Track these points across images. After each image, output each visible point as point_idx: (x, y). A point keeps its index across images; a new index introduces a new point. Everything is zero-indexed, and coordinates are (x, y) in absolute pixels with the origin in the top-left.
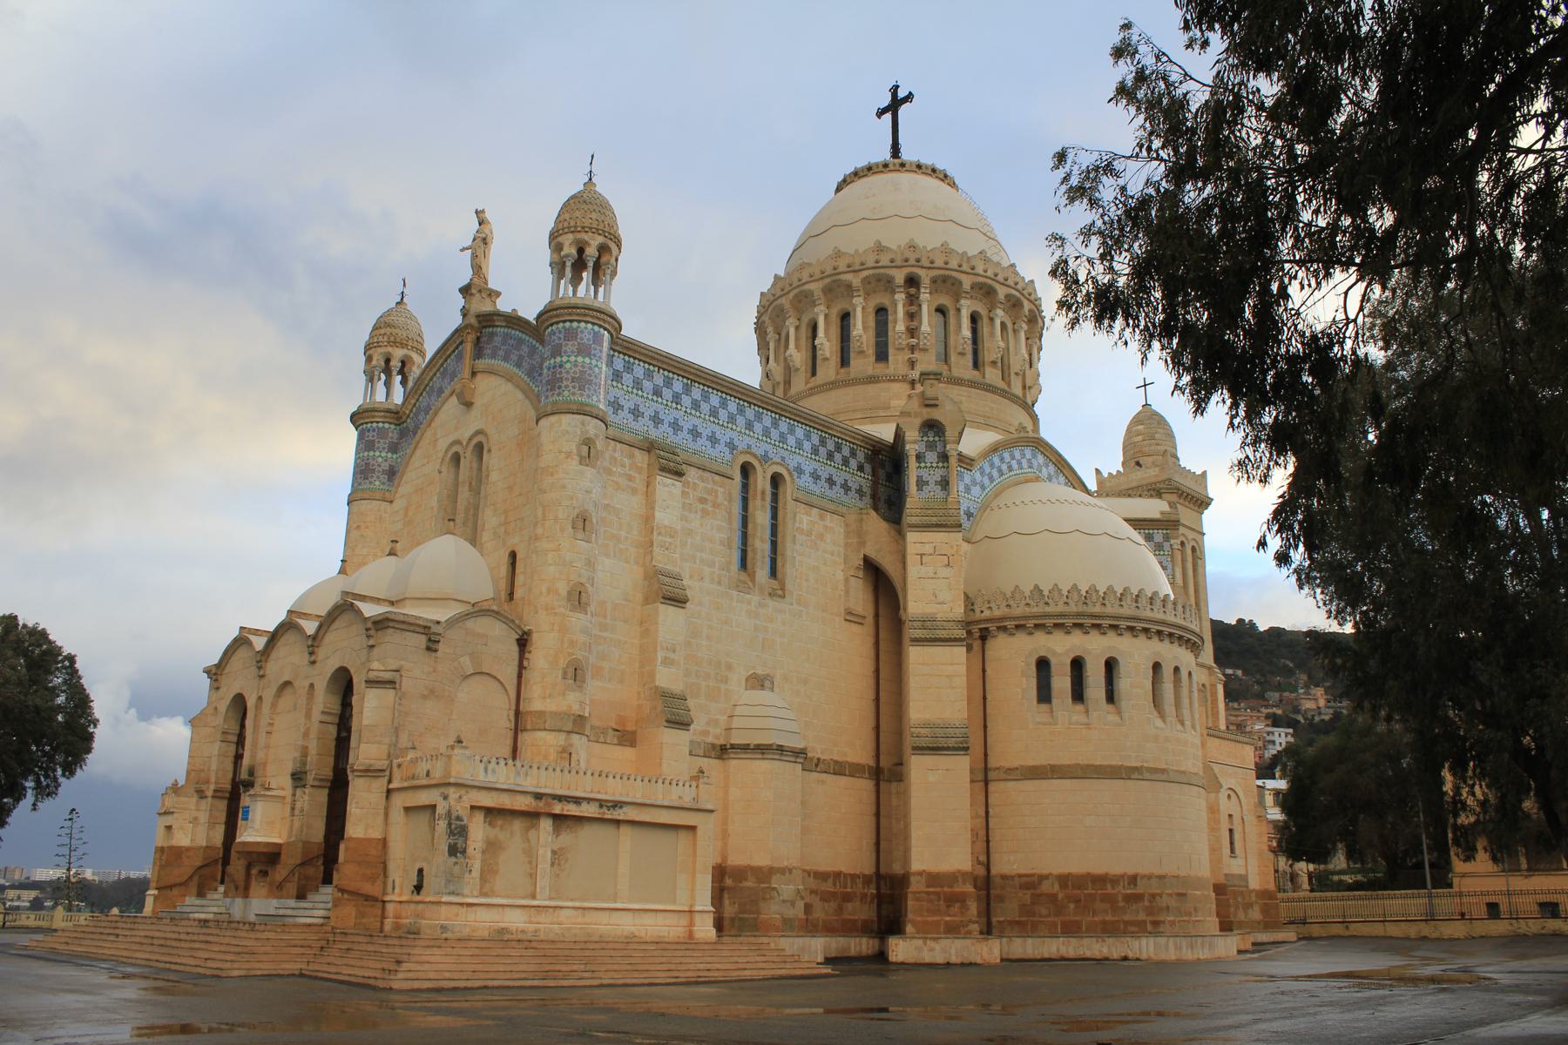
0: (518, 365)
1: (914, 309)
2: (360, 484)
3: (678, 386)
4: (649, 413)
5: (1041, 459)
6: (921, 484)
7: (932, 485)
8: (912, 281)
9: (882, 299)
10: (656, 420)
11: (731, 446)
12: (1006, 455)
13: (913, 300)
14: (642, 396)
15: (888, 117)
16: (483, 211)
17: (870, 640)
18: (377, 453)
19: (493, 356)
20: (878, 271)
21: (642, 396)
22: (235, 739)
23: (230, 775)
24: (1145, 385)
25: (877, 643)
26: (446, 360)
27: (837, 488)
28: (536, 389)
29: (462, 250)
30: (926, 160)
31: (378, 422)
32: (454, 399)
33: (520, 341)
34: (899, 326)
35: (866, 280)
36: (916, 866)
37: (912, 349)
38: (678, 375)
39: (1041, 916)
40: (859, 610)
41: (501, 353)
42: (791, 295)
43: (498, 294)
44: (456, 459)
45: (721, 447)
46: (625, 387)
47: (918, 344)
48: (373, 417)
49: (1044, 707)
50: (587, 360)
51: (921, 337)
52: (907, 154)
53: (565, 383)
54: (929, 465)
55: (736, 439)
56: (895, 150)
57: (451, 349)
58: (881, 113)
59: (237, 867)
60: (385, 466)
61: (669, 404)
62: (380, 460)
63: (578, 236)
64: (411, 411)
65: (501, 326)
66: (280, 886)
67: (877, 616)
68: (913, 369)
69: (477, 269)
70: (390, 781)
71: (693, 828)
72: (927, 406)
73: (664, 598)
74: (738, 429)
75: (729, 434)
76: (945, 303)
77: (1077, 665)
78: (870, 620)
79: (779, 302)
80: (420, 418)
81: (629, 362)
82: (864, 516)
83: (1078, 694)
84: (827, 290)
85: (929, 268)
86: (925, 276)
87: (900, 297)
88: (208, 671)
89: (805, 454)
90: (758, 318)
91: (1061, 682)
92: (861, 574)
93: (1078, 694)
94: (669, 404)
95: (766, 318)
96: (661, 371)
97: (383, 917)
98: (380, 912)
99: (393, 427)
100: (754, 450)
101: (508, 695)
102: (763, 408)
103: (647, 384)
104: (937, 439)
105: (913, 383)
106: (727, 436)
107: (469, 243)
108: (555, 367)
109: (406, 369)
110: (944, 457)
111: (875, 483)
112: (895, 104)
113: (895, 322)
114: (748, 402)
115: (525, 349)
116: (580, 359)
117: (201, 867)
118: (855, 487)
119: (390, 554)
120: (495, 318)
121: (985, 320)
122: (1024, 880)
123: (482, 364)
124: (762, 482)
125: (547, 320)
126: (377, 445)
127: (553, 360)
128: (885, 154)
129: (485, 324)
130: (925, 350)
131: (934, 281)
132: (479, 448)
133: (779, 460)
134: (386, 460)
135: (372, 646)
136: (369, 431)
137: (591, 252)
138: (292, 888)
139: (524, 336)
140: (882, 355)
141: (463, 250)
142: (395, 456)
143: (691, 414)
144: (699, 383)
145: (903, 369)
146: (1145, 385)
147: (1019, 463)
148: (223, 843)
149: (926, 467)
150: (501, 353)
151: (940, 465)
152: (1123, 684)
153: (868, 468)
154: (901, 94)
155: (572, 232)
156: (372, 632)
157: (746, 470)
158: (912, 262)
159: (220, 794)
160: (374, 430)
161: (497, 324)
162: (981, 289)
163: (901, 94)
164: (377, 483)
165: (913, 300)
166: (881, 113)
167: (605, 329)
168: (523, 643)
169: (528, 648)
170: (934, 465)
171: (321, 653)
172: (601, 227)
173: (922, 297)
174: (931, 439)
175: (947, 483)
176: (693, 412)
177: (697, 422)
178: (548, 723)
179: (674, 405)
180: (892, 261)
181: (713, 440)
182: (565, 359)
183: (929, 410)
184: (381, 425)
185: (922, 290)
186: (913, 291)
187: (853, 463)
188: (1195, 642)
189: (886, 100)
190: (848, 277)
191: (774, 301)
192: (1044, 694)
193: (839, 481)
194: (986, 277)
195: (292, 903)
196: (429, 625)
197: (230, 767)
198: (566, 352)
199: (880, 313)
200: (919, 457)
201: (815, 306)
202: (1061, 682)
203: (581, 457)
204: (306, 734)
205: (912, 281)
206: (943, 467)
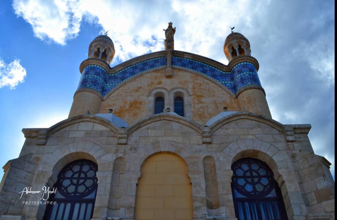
0: (204, 72)
2: (91, 86)
16: (172, 24)
18: (101, 79)
60: (102, 85)
64: (119, 71)
80: (127, 75)
107: (165, 29)
120: (186, 55)
129: (175, 55)
139: (205, 65)
141: (164, 30)
142: (106, 84)
160: (100, 70)
161: (185, 56)
164: (99, 90)
184: (103, 69)
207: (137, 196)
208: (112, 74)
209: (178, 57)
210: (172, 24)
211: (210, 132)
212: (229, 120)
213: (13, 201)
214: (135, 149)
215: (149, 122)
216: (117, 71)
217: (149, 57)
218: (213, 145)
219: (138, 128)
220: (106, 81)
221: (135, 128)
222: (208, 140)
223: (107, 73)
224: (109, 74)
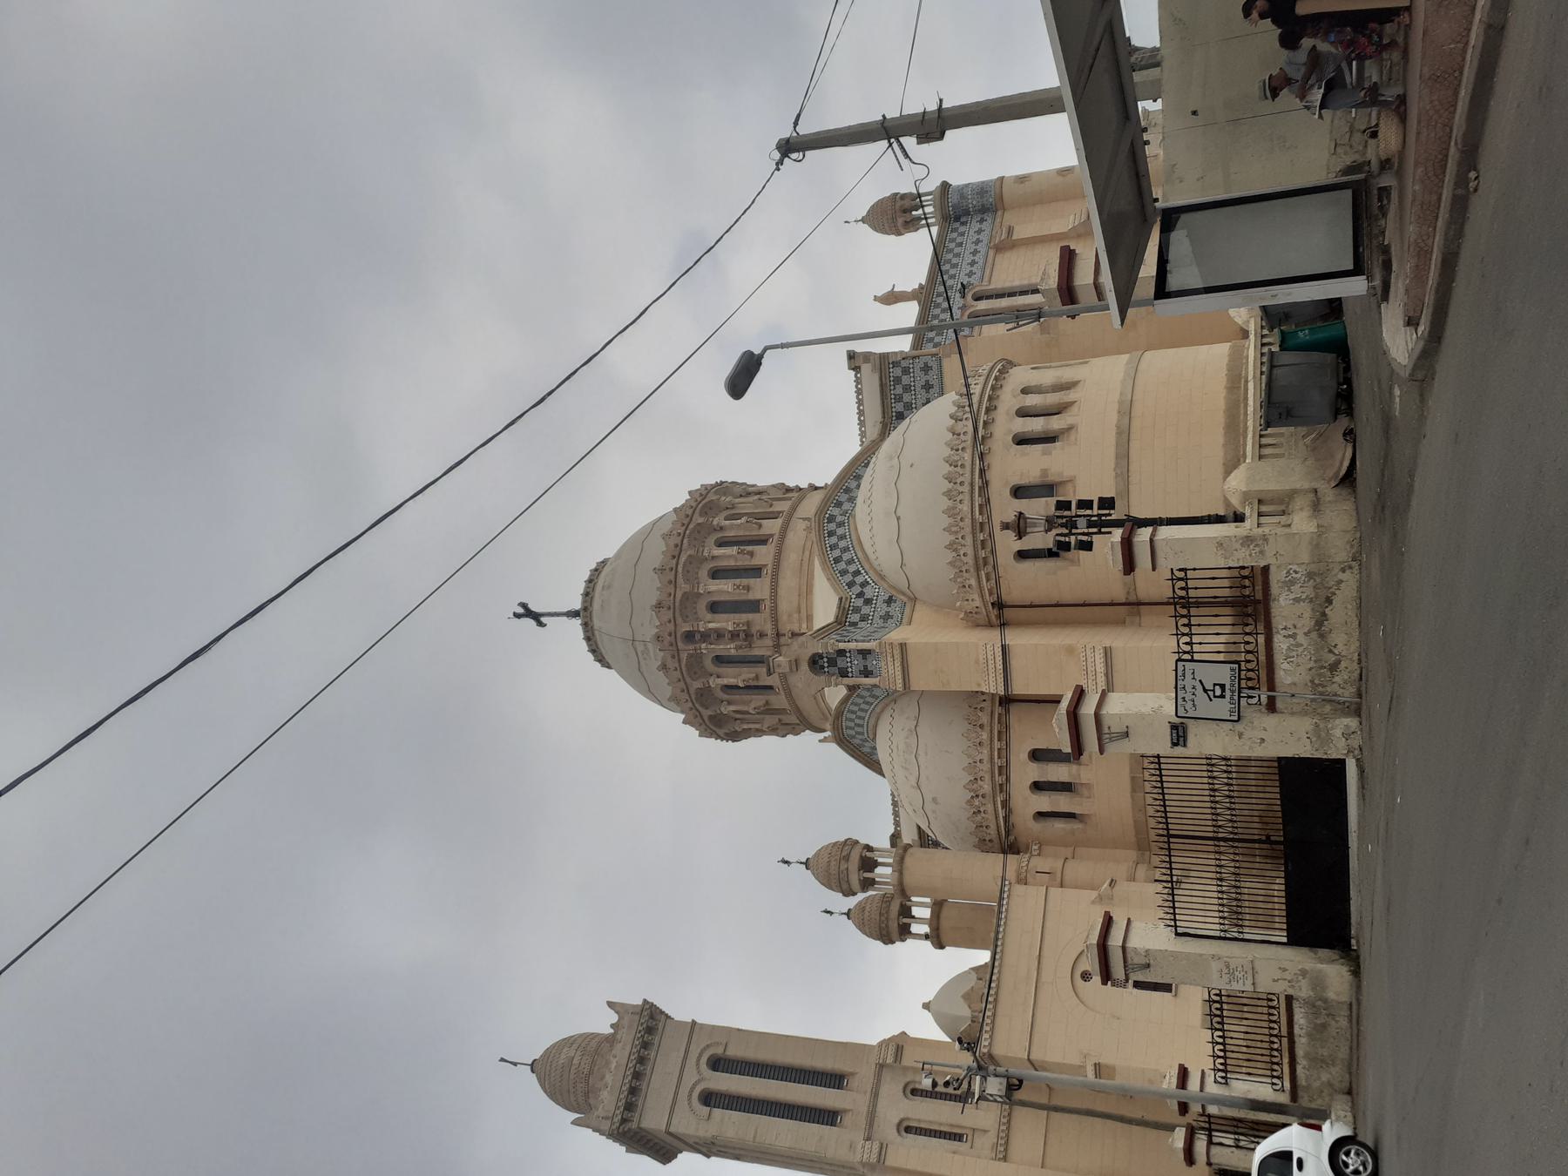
1: (713, 636)
8: (689, 637)
9: (708, 663)
30: (581, 587)
34: (730, 649)
47: (744, 631)
52: (578, 606)
54: (849, 664)
56: (574, 614)
76: (705, 604)
90: (722, 739)
95: (721, 732)
128: (577, 622)
131: (685, 619)
149: (851, 667)
165: (705, 636)
180: (673, 657)
186: (698, 637)
191: (706, 725)
201: (710, 687)
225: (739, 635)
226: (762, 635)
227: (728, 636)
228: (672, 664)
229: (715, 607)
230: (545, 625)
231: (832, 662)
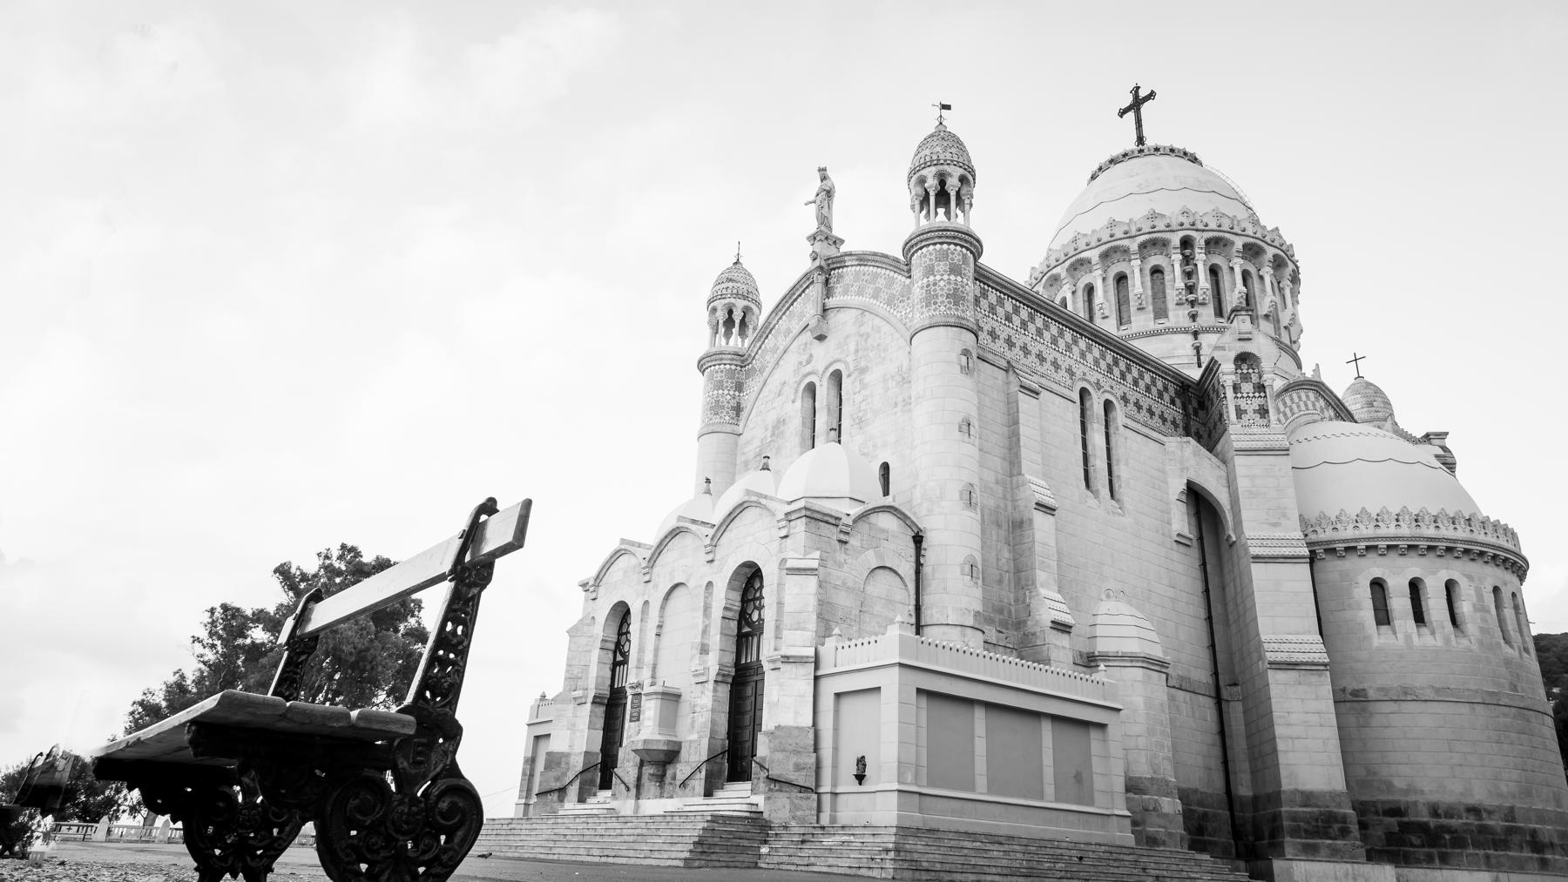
0: (875, 296)
1: (1188, 268)
3: (1024, 313)
4: (1003, 336)
5: (1322, 402)
6: (1240, 412)
7: (1250, 414)
10: (1010, 342)
11: (1070, 372)
12: (1295, 396)
13: (1187, 260)
14: (997, 321)
15: (1131, 115)
16: (824, 170)
17: (1197, 563)
18: (726, 392)
19: (846, 292)
20: (1154, 235)
21: (997, 321)
22: (612, 646)
23: (608, 682)
24: (1356, 360)
25: (1204, 564)
26: (792, 304)
27: (1156, 418)
28: (899, 315)
29: (806, 204)
31: (725, 364)
32: (808, 336)
33: (876, 276)
34: (1175, 281)
35: (1143, 246)
36: (1286, 785)
37: (1192, 303)
38: (1024, 304)
39: (1412, 845)
40: (1186, 532)
41: (855, 289)
42: (1067, 264)
43: (842, 241)
44: (811, 389)
45: (1062, 372)
46: (983, 312)
47: (1196, 299)
48: (721, 359)
49: (1384, 628)
50: (959, 279)
51: (1200, 292)
52: (1150, 142)
53: (940, 299)
54: (1245, 395)
55: (1074, 367)
56: (1140, 140)
57: (797, 294)
58: (1122, 113)
59: (627, 766)
60: (733, 403)
61: (1019, 329)
62: (728, 397)
63: (940, 167)
65: (852, 266)
66: (684, 784)
67: (1201, 539)
68: (1194, 321)
69: (824, 221)
70: (817, 668)
71: (1102, 726)
72: (1240, 340)
73: (1037, 504)
74: (1075, 358)
75: (1069, 361)
77: (1415, 586)
78: (1195, 543)
79: (1055, 271)
80: (767, 358)
81: (984, 289)
82: (1185, 445)
83: (1419, 617)
84: (1105, 256)
85: (1203, 231)
86: (1200, 239)
87: (1177, 257)
88: (584, 585)
89: (1128, 385)
91: (1400, 603)
92: (1184, 498)
93: (1419, 617)
94: (1019, 329)
96: (1010, 299)
97: (819, 810)
98: (815, 805)
99: (739, 368)
100: (1088, 377)
101: (907, 590)
102: (1092, 341)
103: (999, 310)
104: (1251, 371)
105: (1196, 334)
106: (1066, 363)
107: (812, 198)
108: (928, 286)
109: (746, 319)
110: (1261, 388)
111: (1186, 415)
112: (1137, 104)
113: (1174, 280)
114: (1080, 334)
115: (881, 282)
116: (953, 277)
117: (581, 773)
118: (1170, 418)
119: (763, 469)
120: (846, 258)
121: (1255, 279)
122: (1387, 807)
123: (831, 302)
124: (1097, 407)
125: (916, 244)
126: (725, 385)
127: (925, 280)
128: (1131, 144)
129: (832, 266)
130: (1203, 304)
131: (1208, 242)
132: (837, 377)
133: (1109, 389)
134: (734, 398)
135: (786, 537)
136: (717, 372)
137: (952, 184)
138: (699, 783)
140: (1161, 313)
142: (742, 394)
143: (1036, 340)
144: (1041, 313)
145: (1186, 322)
146: (1356, 360)
147: (1306, 405)
148: (601, 750)
149: (1243, 397)
150: (855, 289)
151: (1257, 395)
152: (1465, 607)
153: (1178, 401)
154: (1143, 93)
155: (935, 165)
156: (784, 523)
157: (1084, 393)
158: (1187, 225)
159: (598, 700)
160: (722, 371)
162: (1250, 249)
163: (1143, 93)
164: (727, 418)
166: (1122, 113)
167: (971, 252)
168: (918, 540)
169: (924, 545)
170: (1251, 395)
171: (720, 553)
172: (961, 160)
173: (1197, 256)
174: (1245, 371)
175: (1267, 411)
176: (1038, 338)
177: (1043, 348)
178: (950, 618)
179: (1023, 331)
181: (1056, 366)
182: (938, 278)
183: (1242, 343)
185: (1197, 250)
186: (1188, 252)
187: (1167, 397)
188: (1522, 566)
189: (1129, 100)
190: (1126, 243)
192: (1383, 616)
193: (1157, 413)
194: (1256, 238)
195: (701, 800)
196: (840, 516)
197: (608, 674)
198: (938, 271)
199: (1156, 275)
200: (1236, 388)
202: (1400, 603)
203: (961, 366)
204: (705, 632)
205: (1186, 243)
206: (1260, 397)
207: (657, 650)
208: (748, 364)
209: (839, 268)
210: (824, 170)
211: (710, 545)
212: (733, 516)
213: (580, 675)
214: (656, 586)
215: (668, 540)
216: (753, 355)
217: (794, 294)
218: (716, 563)
219: (660, 553)
220: (739, 387)
221: (657, 554)
222: (710, 557)
223: (742, 367)
224: (745, 366)
225: (1191, 293)
226: (1194, 317)
227: (1190, 282)
228: (1161, 226)
229: (1214, 271)
230: (1121, 117)
231: (1246, 378)
